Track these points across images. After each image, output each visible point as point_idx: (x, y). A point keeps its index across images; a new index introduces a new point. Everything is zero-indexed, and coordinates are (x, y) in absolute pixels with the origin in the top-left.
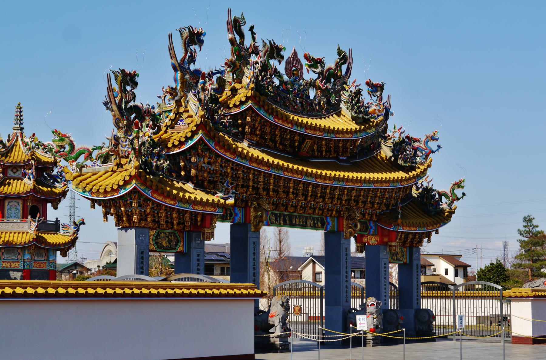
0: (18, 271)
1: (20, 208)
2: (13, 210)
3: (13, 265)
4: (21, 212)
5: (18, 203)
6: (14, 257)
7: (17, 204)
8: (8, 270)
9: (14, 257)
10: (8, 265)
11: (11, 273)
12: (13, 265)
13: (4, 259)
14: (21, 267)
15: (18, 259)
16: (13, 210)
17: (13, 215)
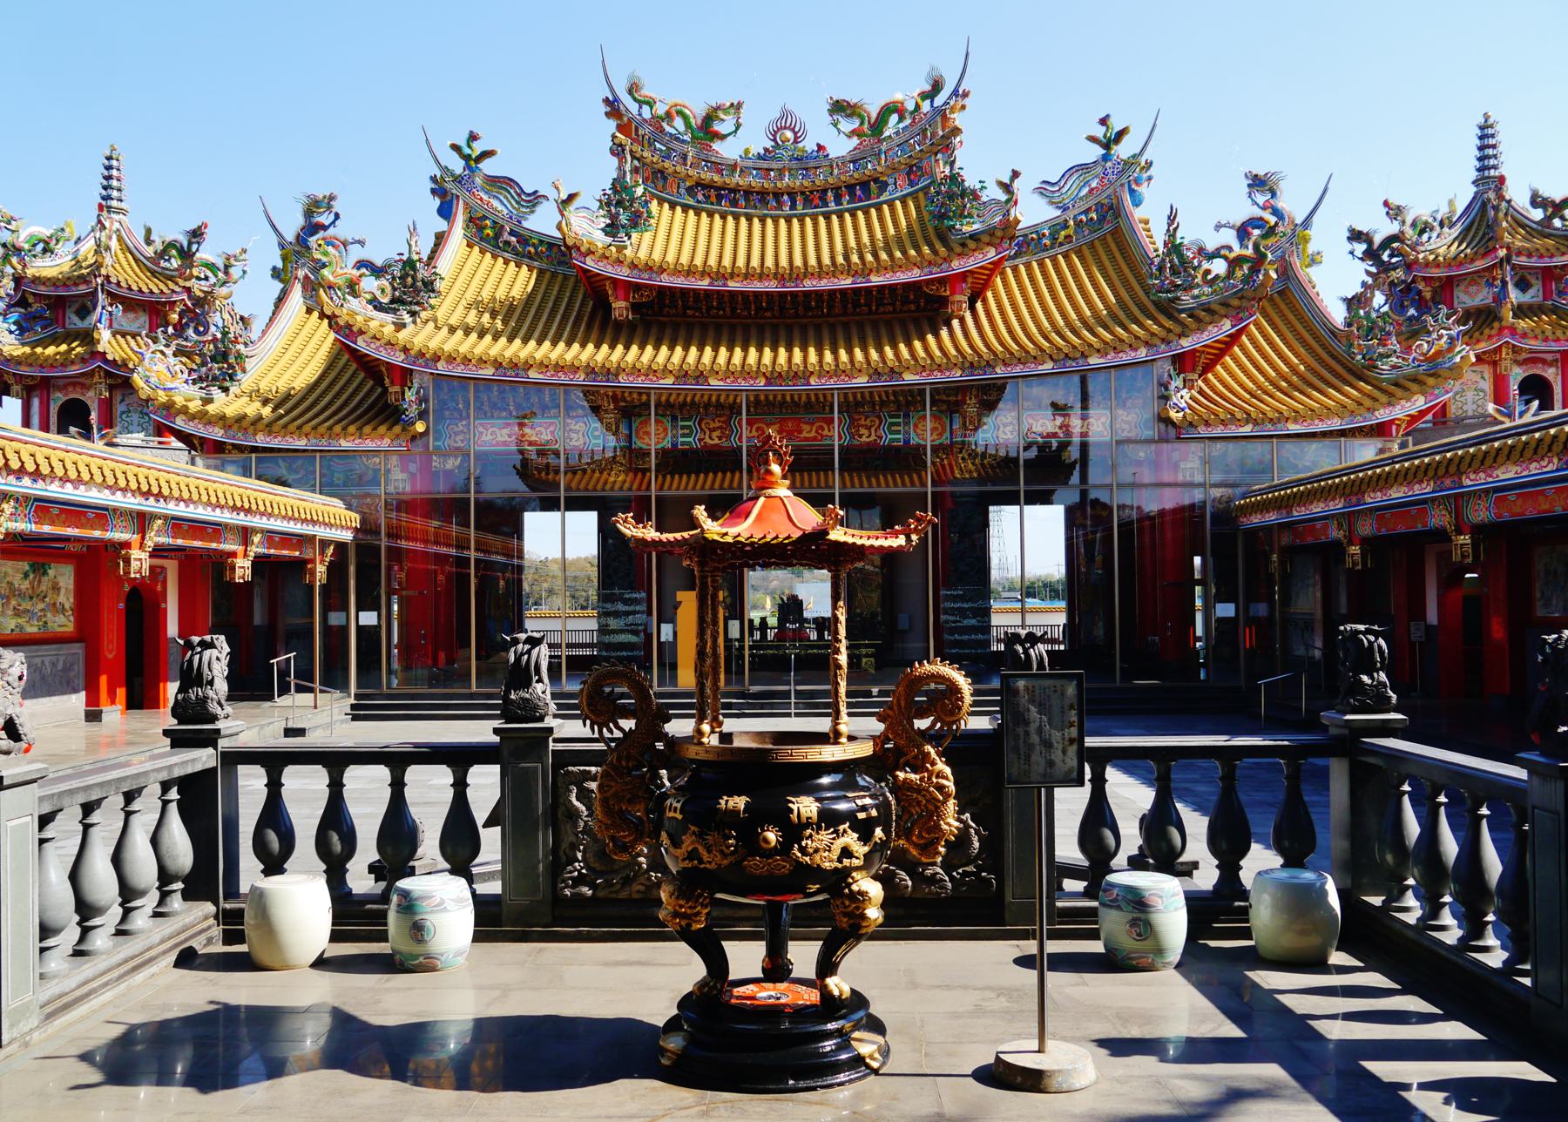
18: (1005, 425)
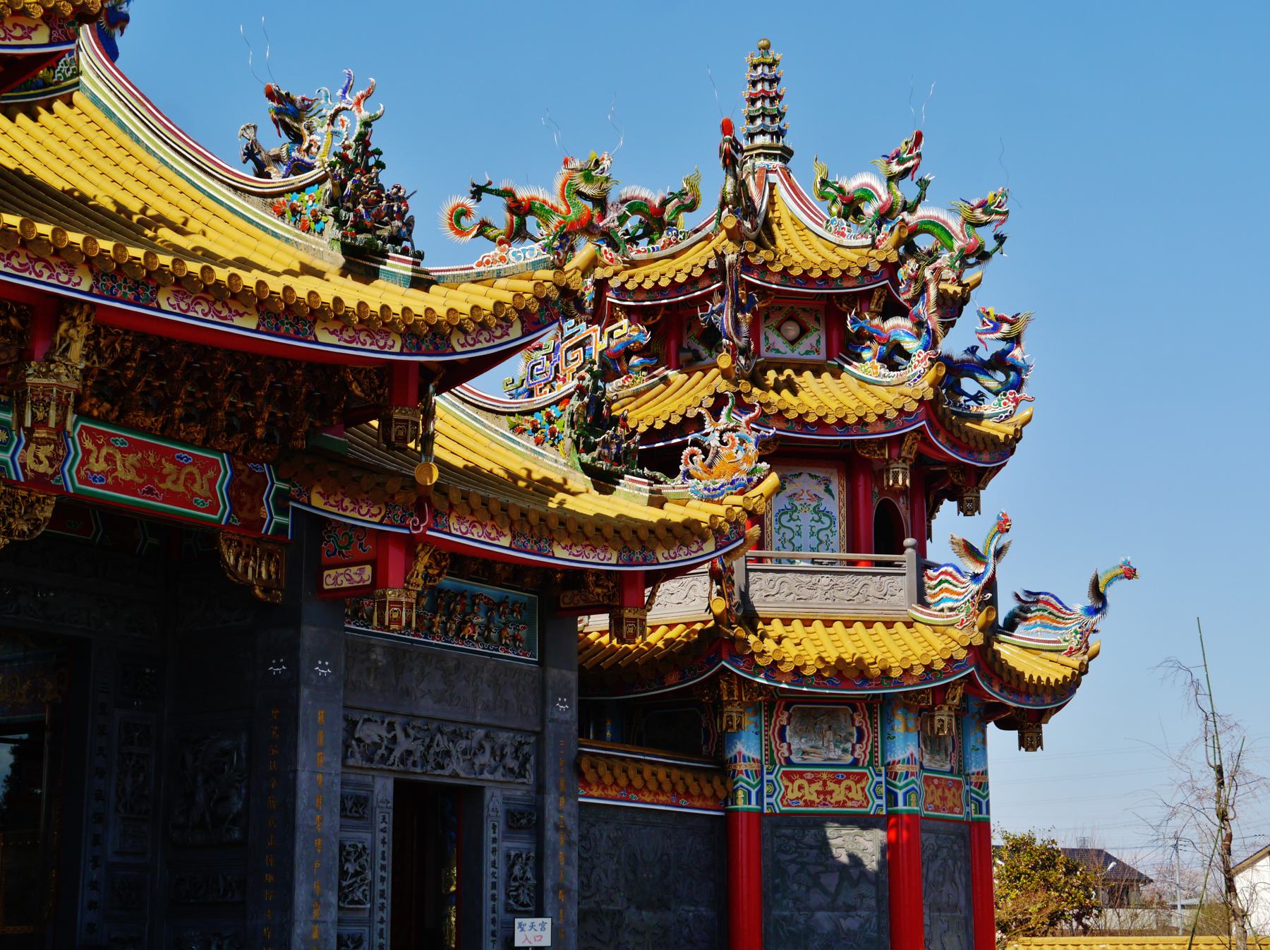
0: (864, 822)
1: (835, 505)
2: (806, 519)
3: (839, 793)
4: (840, 529)
5: (827, 482)
6: (835, 753)
7: (820, 490)
8: (818, 822)
9: (835, 753)
10: (811, 792)
11: (831, 831)
12: (839, 793)
13: (789, 762)
14: (877, 805)
15: (855, 763)
16: (806, 519)
17: (806, 539)
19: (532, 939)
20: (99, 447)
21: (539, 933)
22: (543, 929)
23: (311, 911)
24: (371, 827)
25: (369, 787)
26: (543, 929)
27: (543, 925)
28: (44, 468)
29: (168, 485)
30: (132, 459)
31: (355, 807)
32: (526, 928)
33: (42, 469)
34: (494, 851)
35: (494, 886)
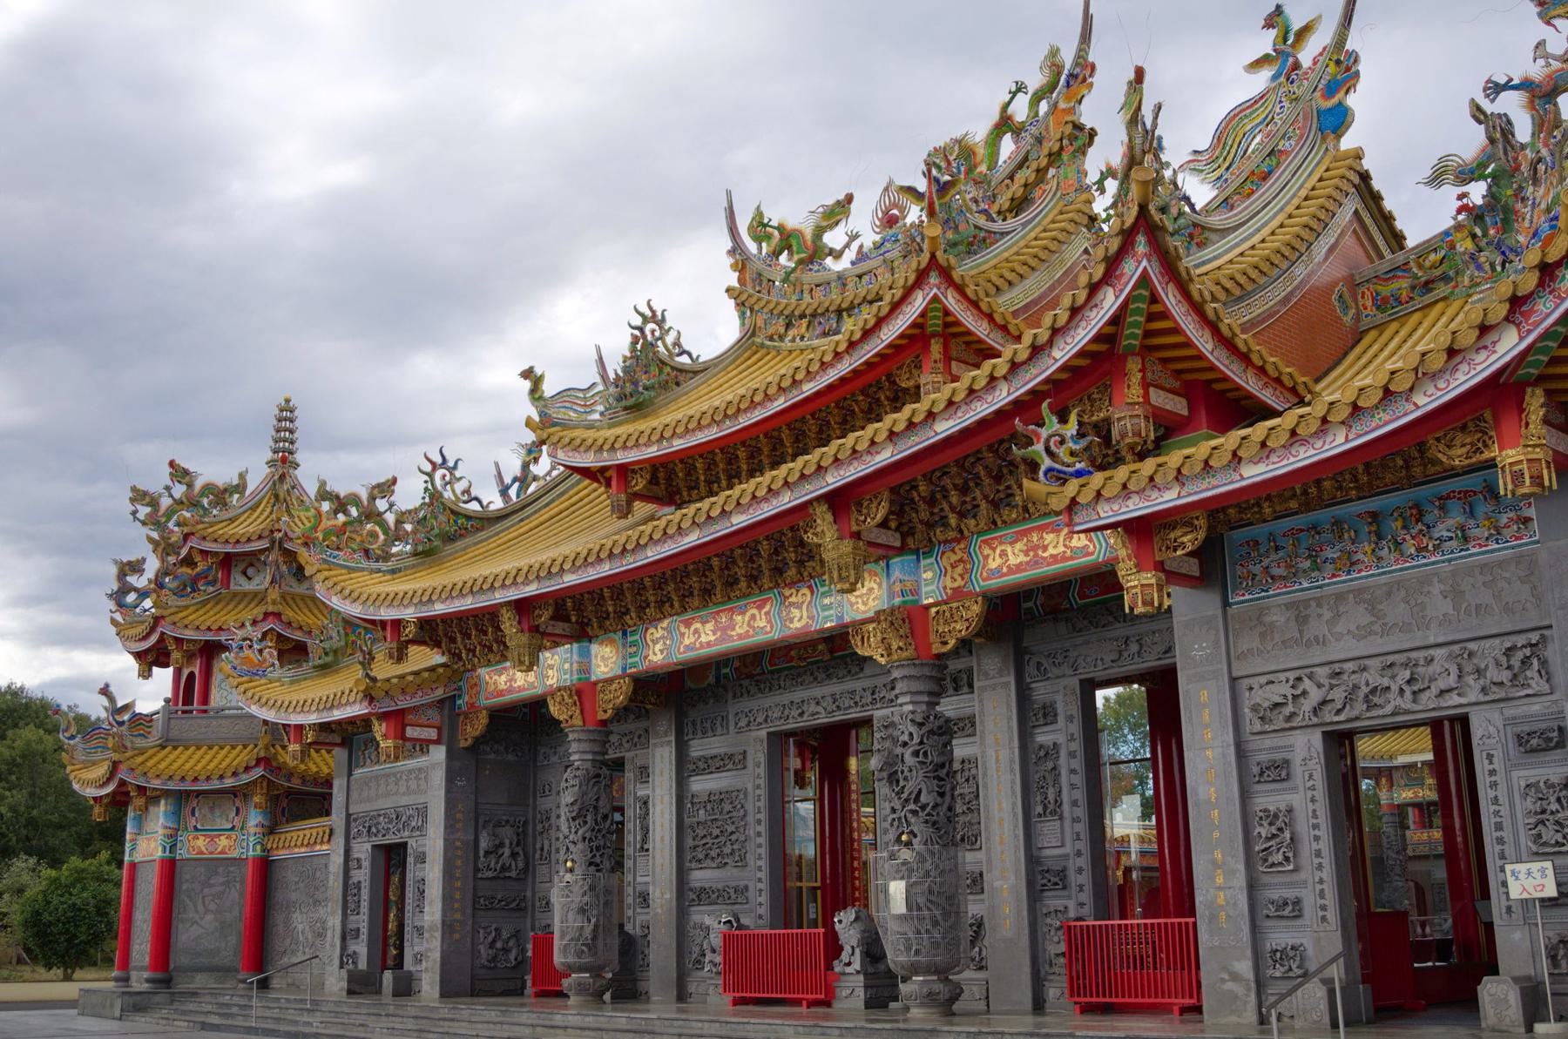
18: (953, 567)
19: (1531, 890)
20: (994, 549)
21: (1539, 881)
22: (1544, 876)
23: (1212, 878)
24: (1295, 789)
25: (1290, 748)
26: (1544, 876)
27: (1543, 870)
28: (959, 582)
29: (1051, 551)
30: (1019, 546)
31: (1256, 772)
32: (1522, 876)
33: (956, 585)
34: (1494, 785)
35: (1499, 827)
